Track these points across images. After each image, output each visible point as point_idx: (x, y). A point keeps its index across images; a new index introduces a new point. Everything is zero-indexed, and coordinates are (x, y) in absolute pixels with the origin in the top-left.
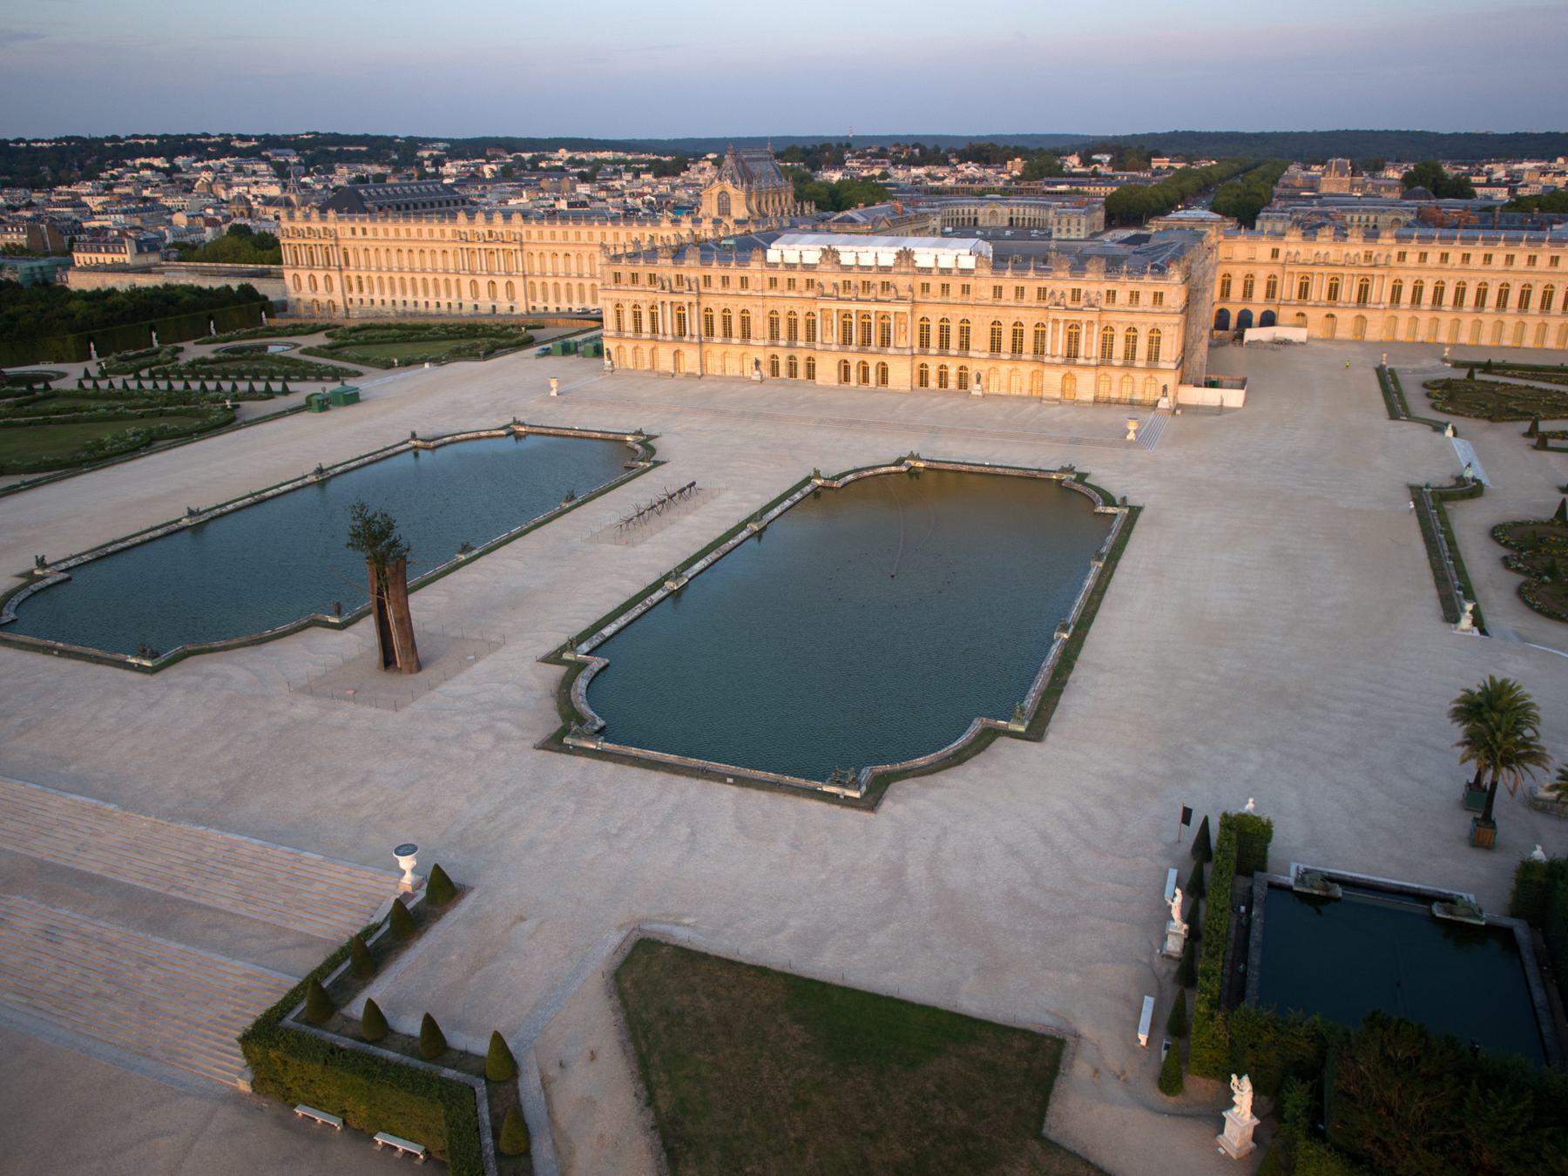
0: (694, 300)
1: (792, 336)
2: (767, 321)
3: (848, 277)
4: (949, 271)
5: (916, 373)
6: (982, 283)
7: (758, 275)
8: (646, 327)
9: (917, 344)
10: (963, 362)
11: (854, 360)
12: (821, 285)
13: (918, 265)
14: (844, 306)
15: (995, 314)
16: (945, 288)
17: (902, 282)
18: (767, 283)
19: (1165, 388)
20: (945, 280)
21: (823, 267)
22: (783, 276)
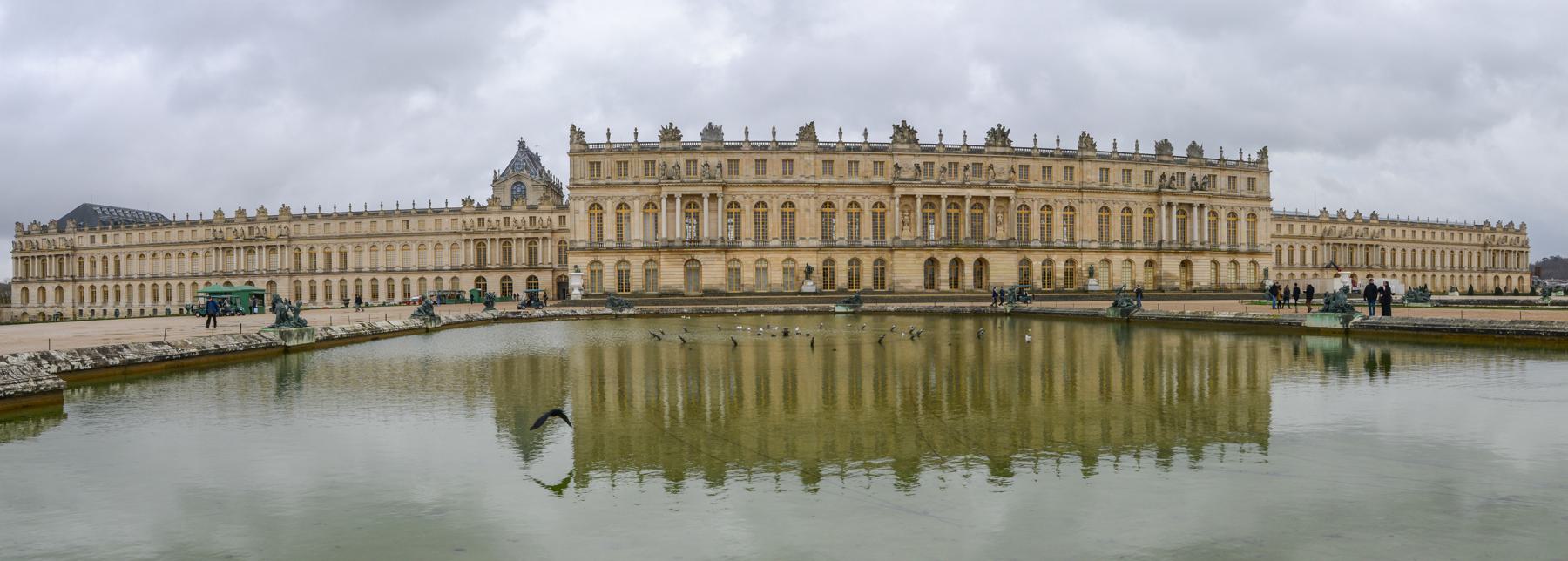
0: (718, 191)
6: (1087, 165)
10: (1075, 255)
12: (897, 167)
15: (1105, 197)
18: (820, 166)
19: (1266, 271)
21: (899, 146)
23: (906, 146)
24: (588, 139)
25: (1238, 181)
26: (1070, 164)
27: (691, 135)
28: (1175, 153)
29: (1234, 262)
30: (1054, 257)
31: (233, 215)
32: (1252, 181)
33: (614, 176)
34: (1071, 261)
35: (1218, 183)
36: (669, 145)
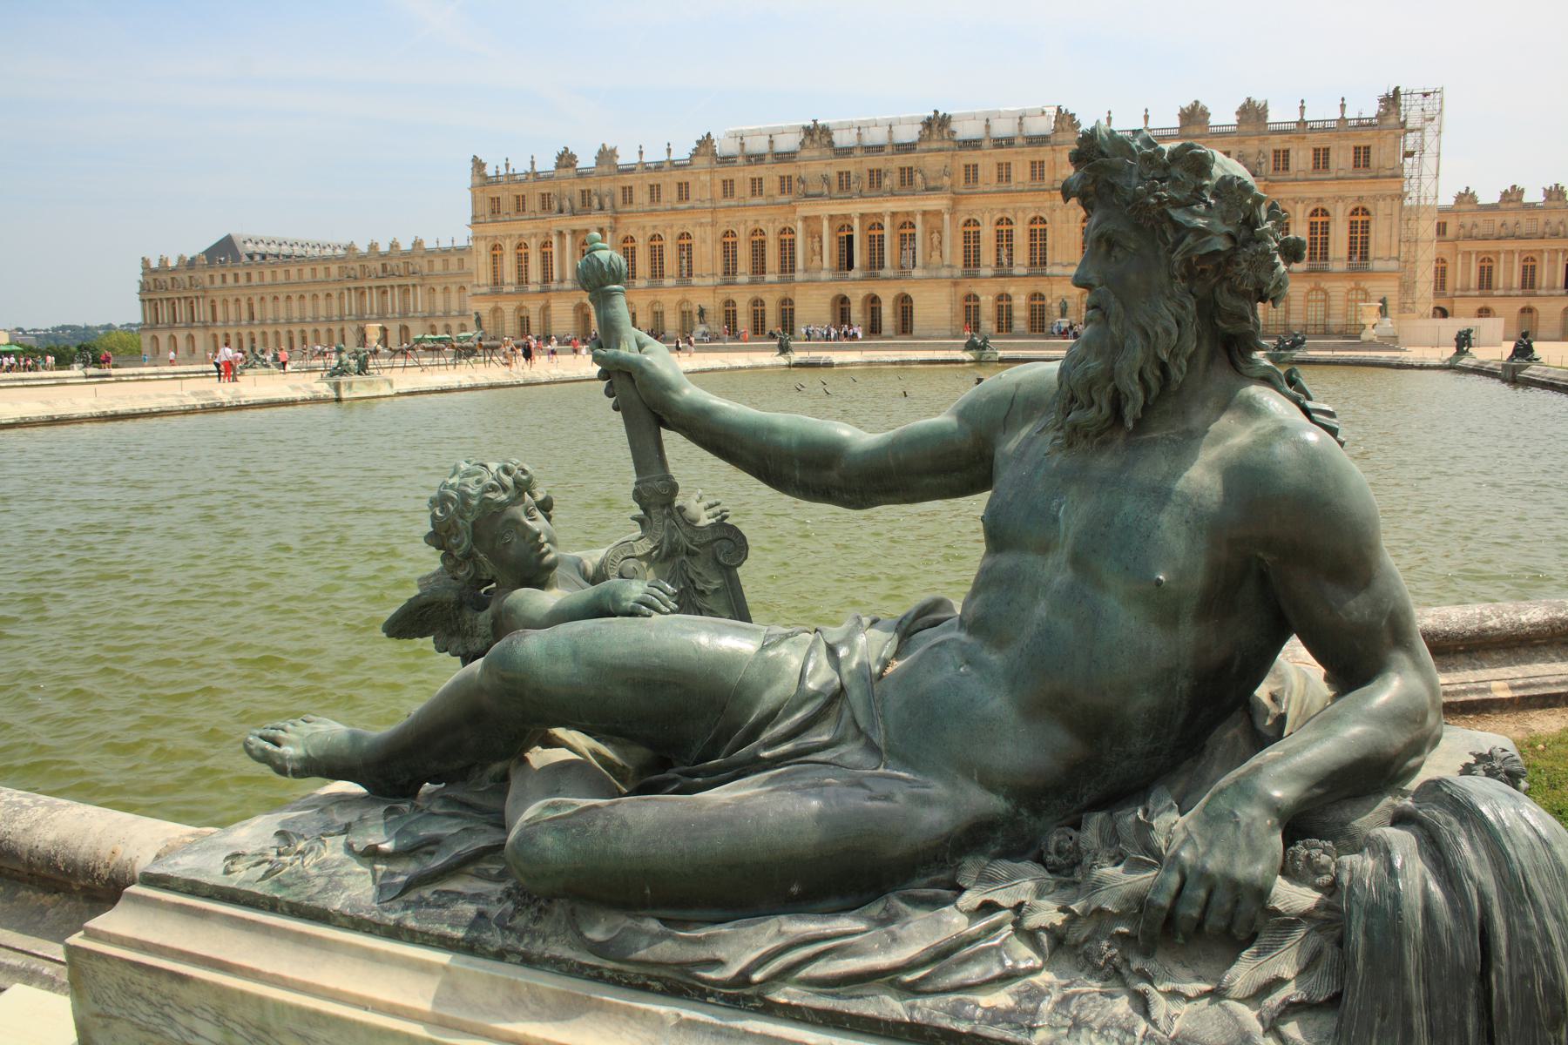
0: (605, 222)
1: (759, 268)
2: (719, 247)
3: (847, 165)
4: (1009, 142)
5: (960, 308)
7: (705, 178)
8: (535, 274)
9: (960, 262)
10: (1042, 286)
11: (857, 295)
12: (801, 181)
13: (960, 136)
14: (837, 209)
16: (1004, 172)
17: (932, 163)
18: (719, 189)
20: (1003, 155)
21: (806, 153)
22: (742, 175)
23: (816, 153)
24: (490, 171)
25: (1332, 156)
26: (1037, 158)
27: (586, 160)
28: (1213, 121)
29: (1317, 289)
30: (1011, 290)
31: (365, 250)
32: (1362, 156)
33: (512, 212)
34: (1036, 296)
35: (1292, 161)
36: (563, 172)
